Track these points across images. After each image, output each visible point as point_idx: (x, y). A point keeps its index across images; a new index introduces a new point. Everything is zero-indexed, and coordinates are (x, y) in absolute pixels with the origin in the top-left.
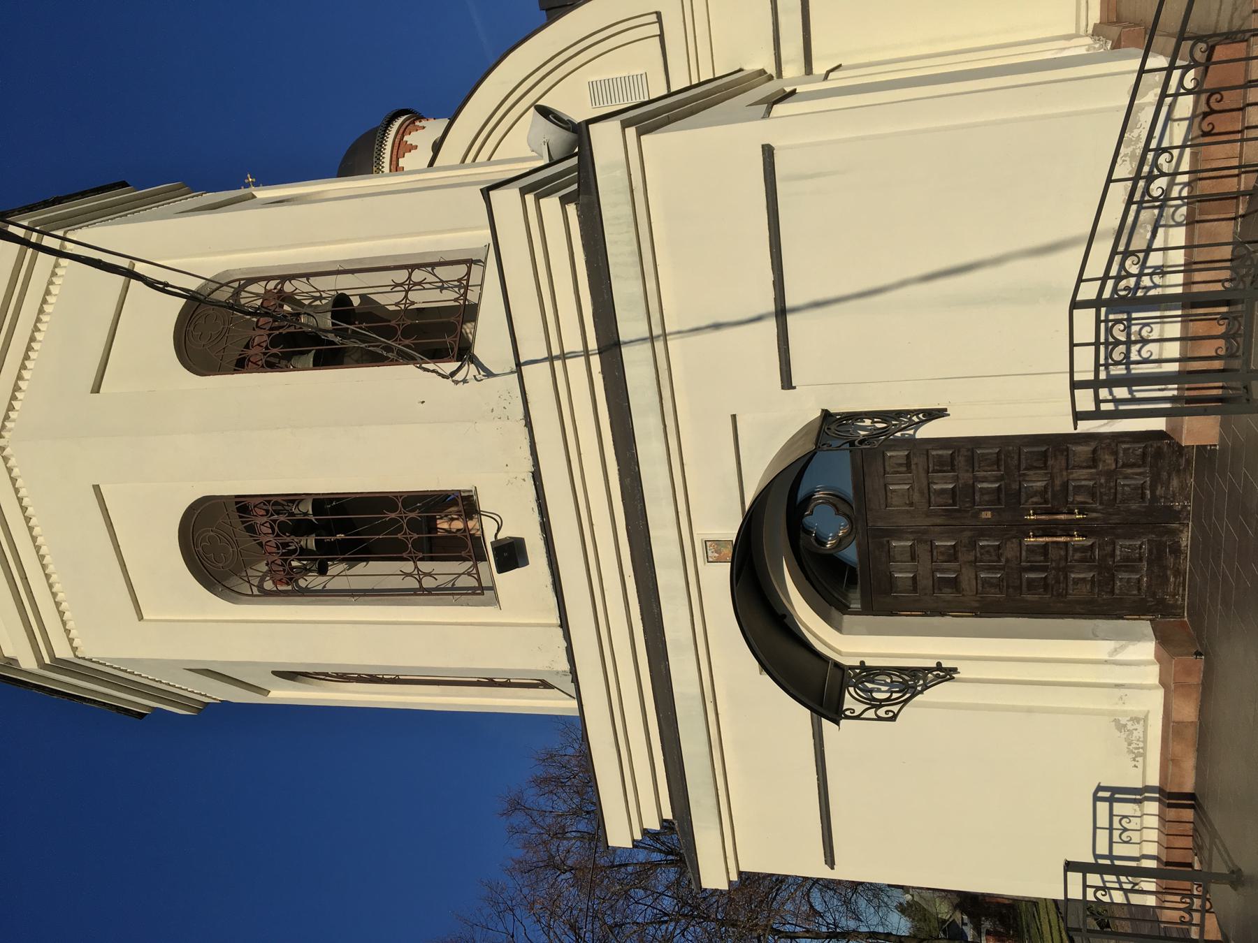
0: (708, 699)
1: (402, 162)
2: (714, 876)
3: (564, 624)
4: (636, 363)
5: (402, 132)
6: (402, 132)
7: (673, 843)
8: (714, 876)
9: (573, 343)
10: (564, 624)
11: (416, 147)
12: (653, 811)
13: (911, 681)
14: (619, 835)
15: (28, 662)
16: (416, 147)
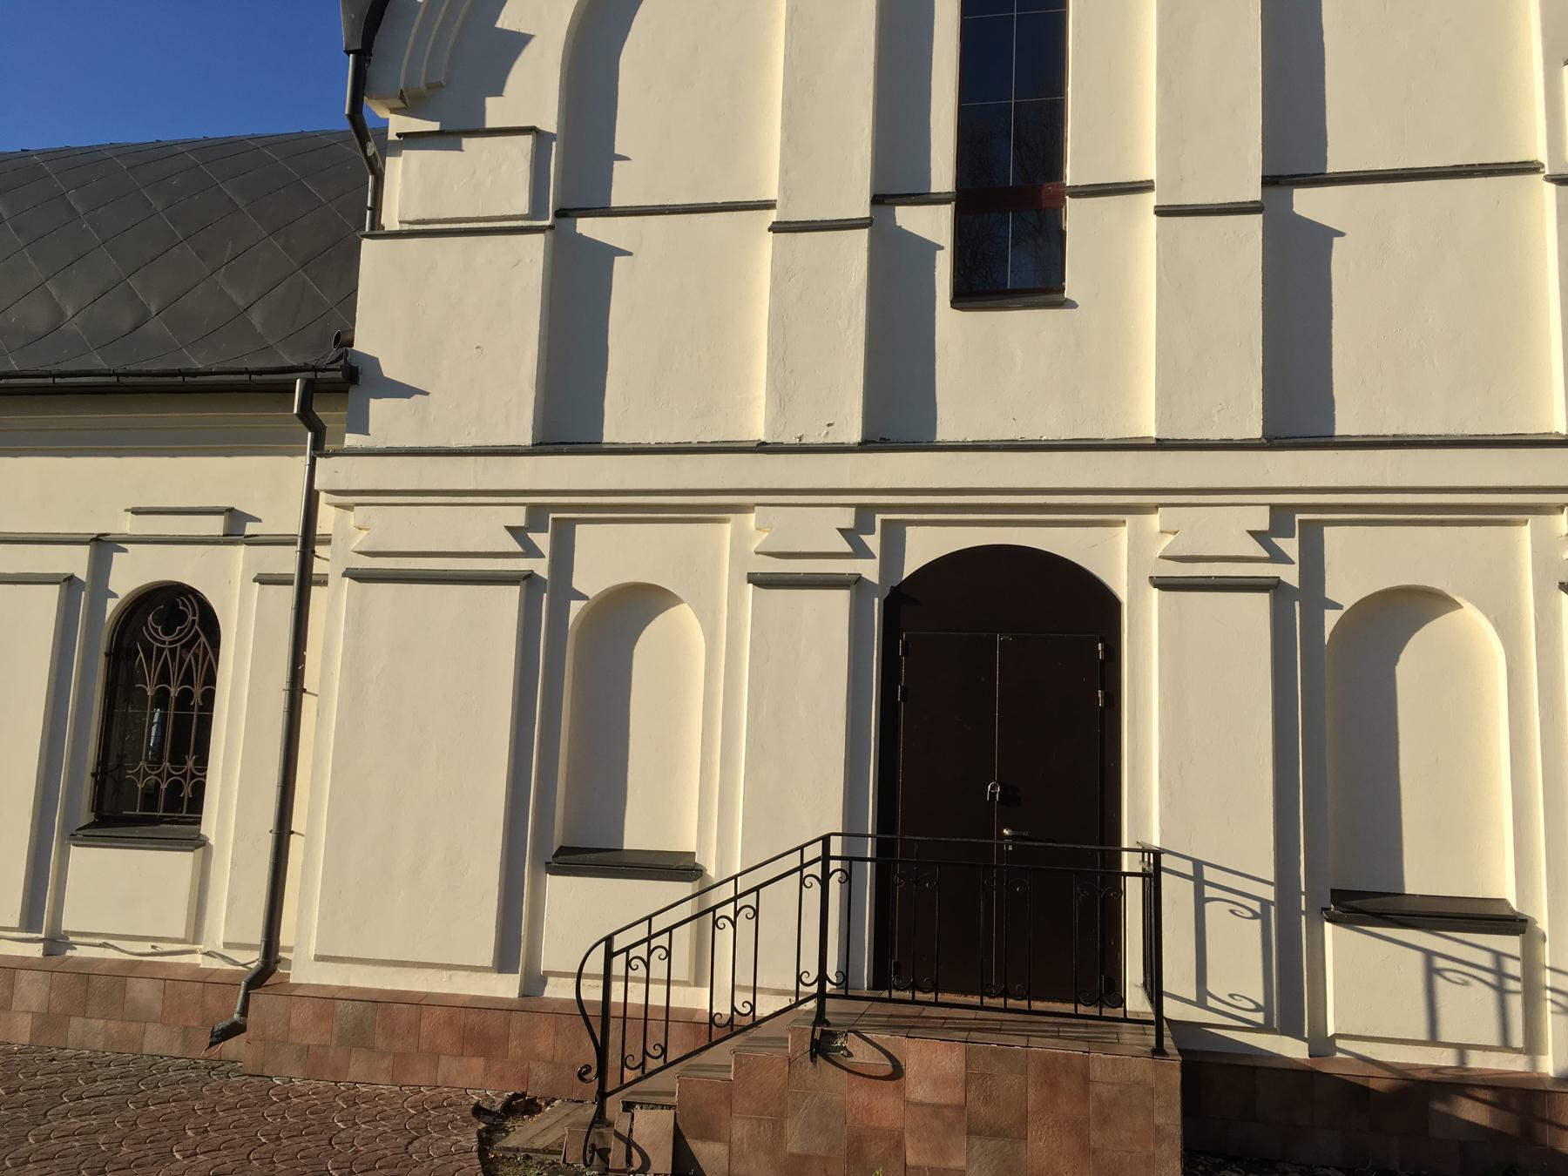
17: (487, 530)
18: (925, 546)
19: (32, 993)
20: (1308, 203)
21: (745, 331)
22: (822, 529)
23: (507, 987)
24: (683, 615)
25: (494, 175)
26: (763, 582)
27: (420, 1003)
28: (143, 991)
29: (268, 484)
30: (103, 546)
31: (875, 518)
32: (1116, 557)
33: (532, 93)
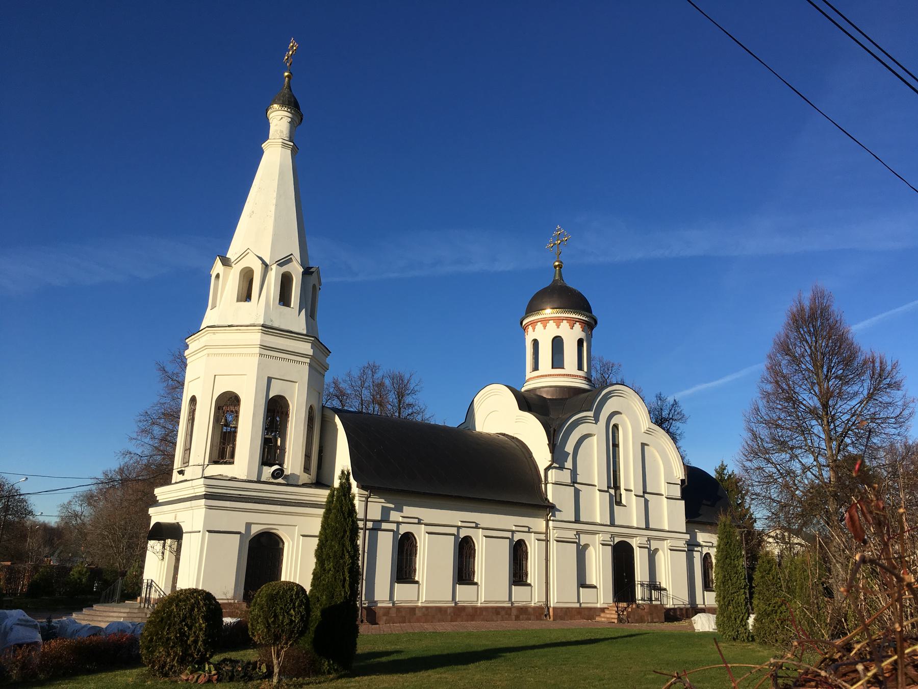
0: (164, 513)
1: (551, 322)
2: (151, 511)
3: (176, 483)
4: (188, 504)
5: (567, 319)
6: (567, 319)
7: (154, 502)
8: (151, 511)
9: (196, 491)
10: (176, 483)
11: (558, 327)
12: (160, 498)
13: (163, 553)
14: (158, 491)
15: (187, 353)
16: (558, 327)
17: (571, 535)
18: (617, 540)
19: (514, 612)
20: (646, 496)
21: (596, 506)
22: (607, 537)
23: (578, 605)
24: (591, 549)
25: (566, 476)
26: (603, 545)
27: (572, 608)
28: (530, 610)
29: (539, 524)
30: (513, 532)
31: (613, 536)
32: (634, 543)
33: (569, 464)
